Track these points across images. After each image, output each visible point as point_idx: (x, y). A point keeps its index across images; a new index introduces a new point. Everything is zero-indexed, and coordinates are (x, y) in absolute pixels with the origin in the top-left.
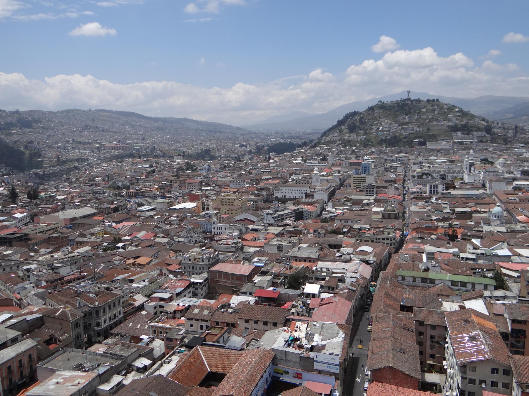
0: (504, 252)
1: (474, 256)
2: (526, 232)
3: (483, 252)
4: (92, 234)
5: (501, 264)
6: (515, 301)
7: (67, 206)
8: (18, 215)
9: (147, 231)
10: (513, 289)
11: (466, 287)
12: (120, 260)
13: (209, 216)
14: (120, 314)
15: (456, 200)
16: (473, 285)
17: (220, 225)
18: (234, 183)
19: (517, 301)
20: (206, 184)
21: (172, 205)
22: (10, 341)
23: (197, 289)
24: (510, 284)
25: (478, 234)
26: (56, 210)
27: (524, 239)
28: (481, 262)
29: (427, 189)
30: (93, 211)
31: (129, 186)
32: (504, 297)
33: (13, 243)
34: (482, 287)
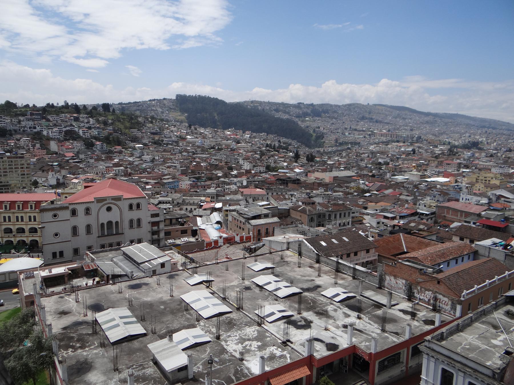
4: (347, 187)
7: (334, 169)
8: (297, 170)
9: (395, 190)
12: (364, 202)
13: (459, 188)
14: (348, 224)
17: (469, 197)
18: (497, 168)
20: (465, 166)
21: (425, 178)
22: (263, 215)
23: (422, 219)
26: (324, 171)
30: (354, 174)
31: (389, 163)
33: (289, 184)
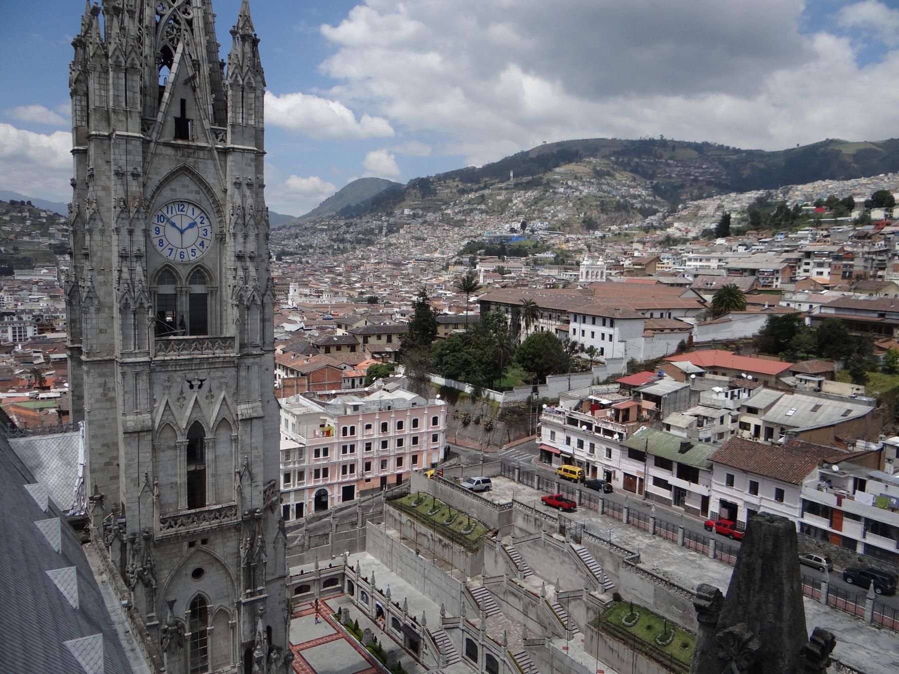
15: (55, 345)
29: (9, 336)
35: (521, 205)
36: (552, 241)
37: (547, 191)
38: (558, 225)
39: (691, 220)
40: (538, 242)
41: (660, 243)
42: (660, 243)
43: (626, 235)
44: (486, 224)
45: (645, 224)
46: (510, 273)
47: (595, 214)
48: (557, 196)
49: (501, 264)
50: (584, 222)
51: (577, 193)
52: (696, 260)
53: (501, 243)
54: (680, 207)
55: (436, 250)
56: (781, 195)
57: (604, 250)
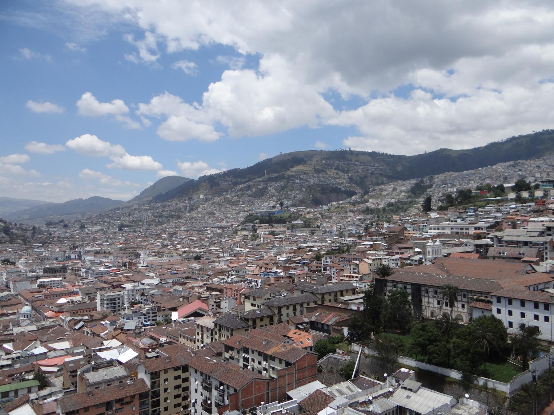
0: (40, 350)
1: (9, 362)
2: (56, 326)
3: (19, 355)
5: (40, 362)
6: (61, 395)
10: (56, 384)
11: (8, 396)
16: (16, 392)
19: (63, 394)
24: (53, 380)
25: (9, 337)
27: (55, 333)
28: (17, 366)
32: (50, 395)
34: (26, 391)
35: (274, 191)
36: (300, 213)
37: (289, 182)
38: (298, 203)
39: (378, 198)
40: (291, 214)
41: (363, 212)
42: (363, 212)
43: (342, 208)
44: (252, 203)
45: (352, 201)
46: (279, 235)
47: (318, 195)
48: (295, 185)
49: (273, 229)
50: (313, 200)
51: (307, 183)
52: (435, 229)
53: (269, 216)
54: (371, 189)
55: (223, 220)
56: (428, 181)
57: (331, 218)
